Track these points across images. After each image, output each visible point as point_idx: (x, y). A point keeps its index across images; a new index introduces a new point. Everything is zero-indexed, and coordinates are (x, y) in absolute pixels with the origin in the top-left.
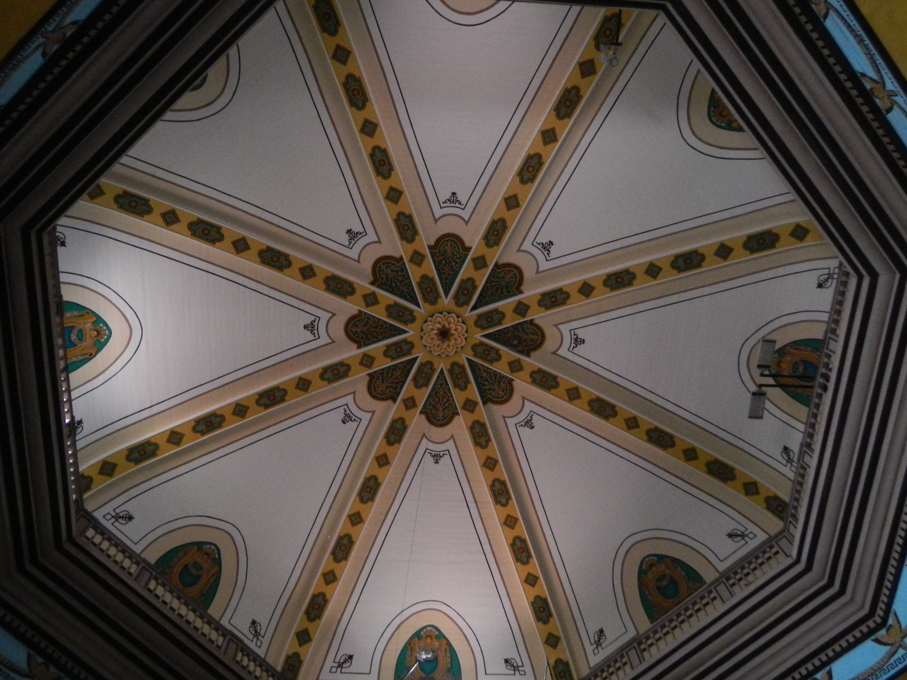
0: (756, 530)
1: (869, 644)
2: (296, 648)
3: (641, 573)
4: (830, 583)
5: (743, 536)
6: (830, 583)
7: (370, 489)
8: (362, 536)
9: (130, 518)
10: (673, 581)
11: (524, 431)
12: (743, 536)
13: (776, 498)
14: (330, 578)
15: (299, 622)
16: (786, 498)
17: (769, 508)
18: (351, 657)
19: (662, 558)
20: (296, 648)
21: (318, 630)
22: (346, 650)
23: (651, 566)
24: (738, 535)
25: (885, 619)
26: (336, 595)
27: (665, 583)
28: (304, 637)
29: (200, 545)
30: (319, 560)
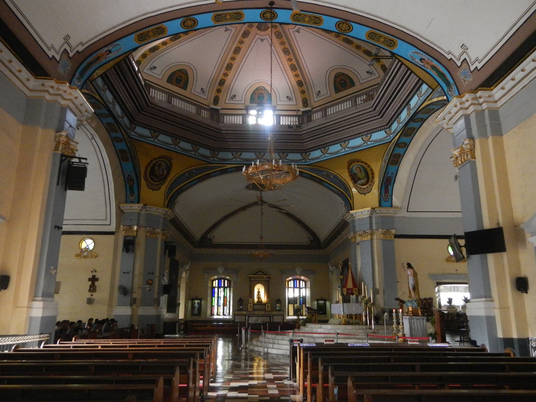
0: (376, 73)
1: (383, 132)
2: (217, 94)
3: (336, 77)
4: (379, 114)
5: (371, 73)
6: (379, 114)
7: (237, 51)
8: (235, 64)
9: (155, 68)
10: (345, 81)
11: (296, 34)
12: (371, 73)
13: (385, 66)
14: (226, 75)
15: (217, 86)
16: (387, 67)
17: (382, 68)
18: (235, 96)
19: (343, 74)
20: (217, 94)
21: (223, 89)
22: (233, 94)
23: (339, 76)
24: (370, 73)
25: (389, 127)
26: (228, 80)
27: (343, 82)
28: (219, 91)
29: (180, 70)
30: (221, 70)
